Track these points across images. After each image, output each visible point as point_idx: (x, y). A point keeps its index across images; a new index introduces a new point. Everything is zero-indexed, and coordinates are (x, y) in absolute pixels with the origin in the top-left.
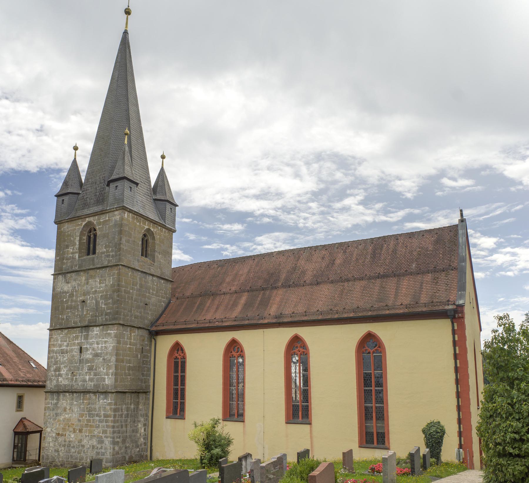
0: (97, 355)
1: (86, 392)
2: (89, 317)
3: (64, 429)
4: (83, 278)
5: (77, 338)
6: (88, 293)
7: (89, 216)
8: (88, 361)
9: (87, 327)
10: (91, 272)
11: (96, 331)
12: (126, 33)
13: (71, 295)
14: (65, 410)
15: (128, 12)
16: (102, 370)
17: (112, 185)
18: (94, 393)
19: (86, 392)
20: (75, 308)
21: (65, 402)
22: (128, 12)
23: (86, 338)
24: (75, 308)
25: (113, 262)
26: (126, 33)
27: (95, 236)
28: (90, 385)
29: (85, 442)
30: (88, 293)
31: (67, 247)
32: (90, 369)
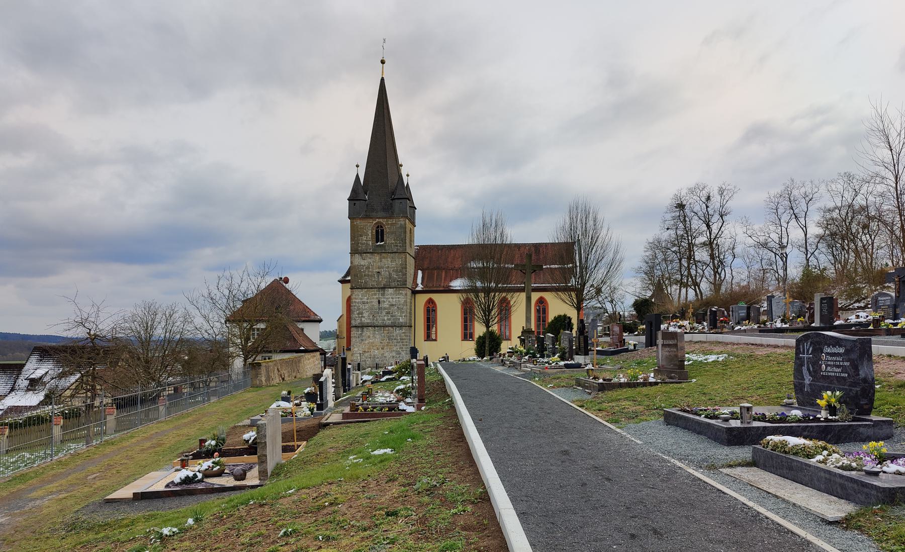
0: (392, 305)
1: (385, 326)
2: (384, 282)
3: (369, 348)
4: (377, 257)
5: (375, 294)
6: (382, 267)
7: (379, 218)
8: (385, 309)
9: (384, 288)
10: (384, 255)
11: (391, 291)
12: (382, 79)
13: (368, 268)
14: (369, 337)
15: (383, 62)
16: (397, 314)
17: (397, 202)
18: (392, 327)
19: (385, 326)
20: (372, 276)
21: (368, 332)
22: (383, 62)
23: (383, 295)
24: (372, 276)
25: (401, 250)
26: (382, 79)
27: (382, 231)
28: (388, 322)
29: (386, 354)
30: (382, 267)
31: (361, 236)
32: (388, 313)
